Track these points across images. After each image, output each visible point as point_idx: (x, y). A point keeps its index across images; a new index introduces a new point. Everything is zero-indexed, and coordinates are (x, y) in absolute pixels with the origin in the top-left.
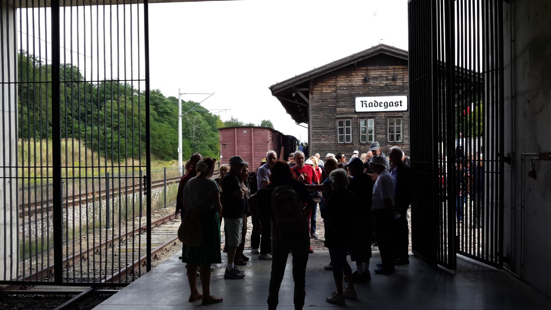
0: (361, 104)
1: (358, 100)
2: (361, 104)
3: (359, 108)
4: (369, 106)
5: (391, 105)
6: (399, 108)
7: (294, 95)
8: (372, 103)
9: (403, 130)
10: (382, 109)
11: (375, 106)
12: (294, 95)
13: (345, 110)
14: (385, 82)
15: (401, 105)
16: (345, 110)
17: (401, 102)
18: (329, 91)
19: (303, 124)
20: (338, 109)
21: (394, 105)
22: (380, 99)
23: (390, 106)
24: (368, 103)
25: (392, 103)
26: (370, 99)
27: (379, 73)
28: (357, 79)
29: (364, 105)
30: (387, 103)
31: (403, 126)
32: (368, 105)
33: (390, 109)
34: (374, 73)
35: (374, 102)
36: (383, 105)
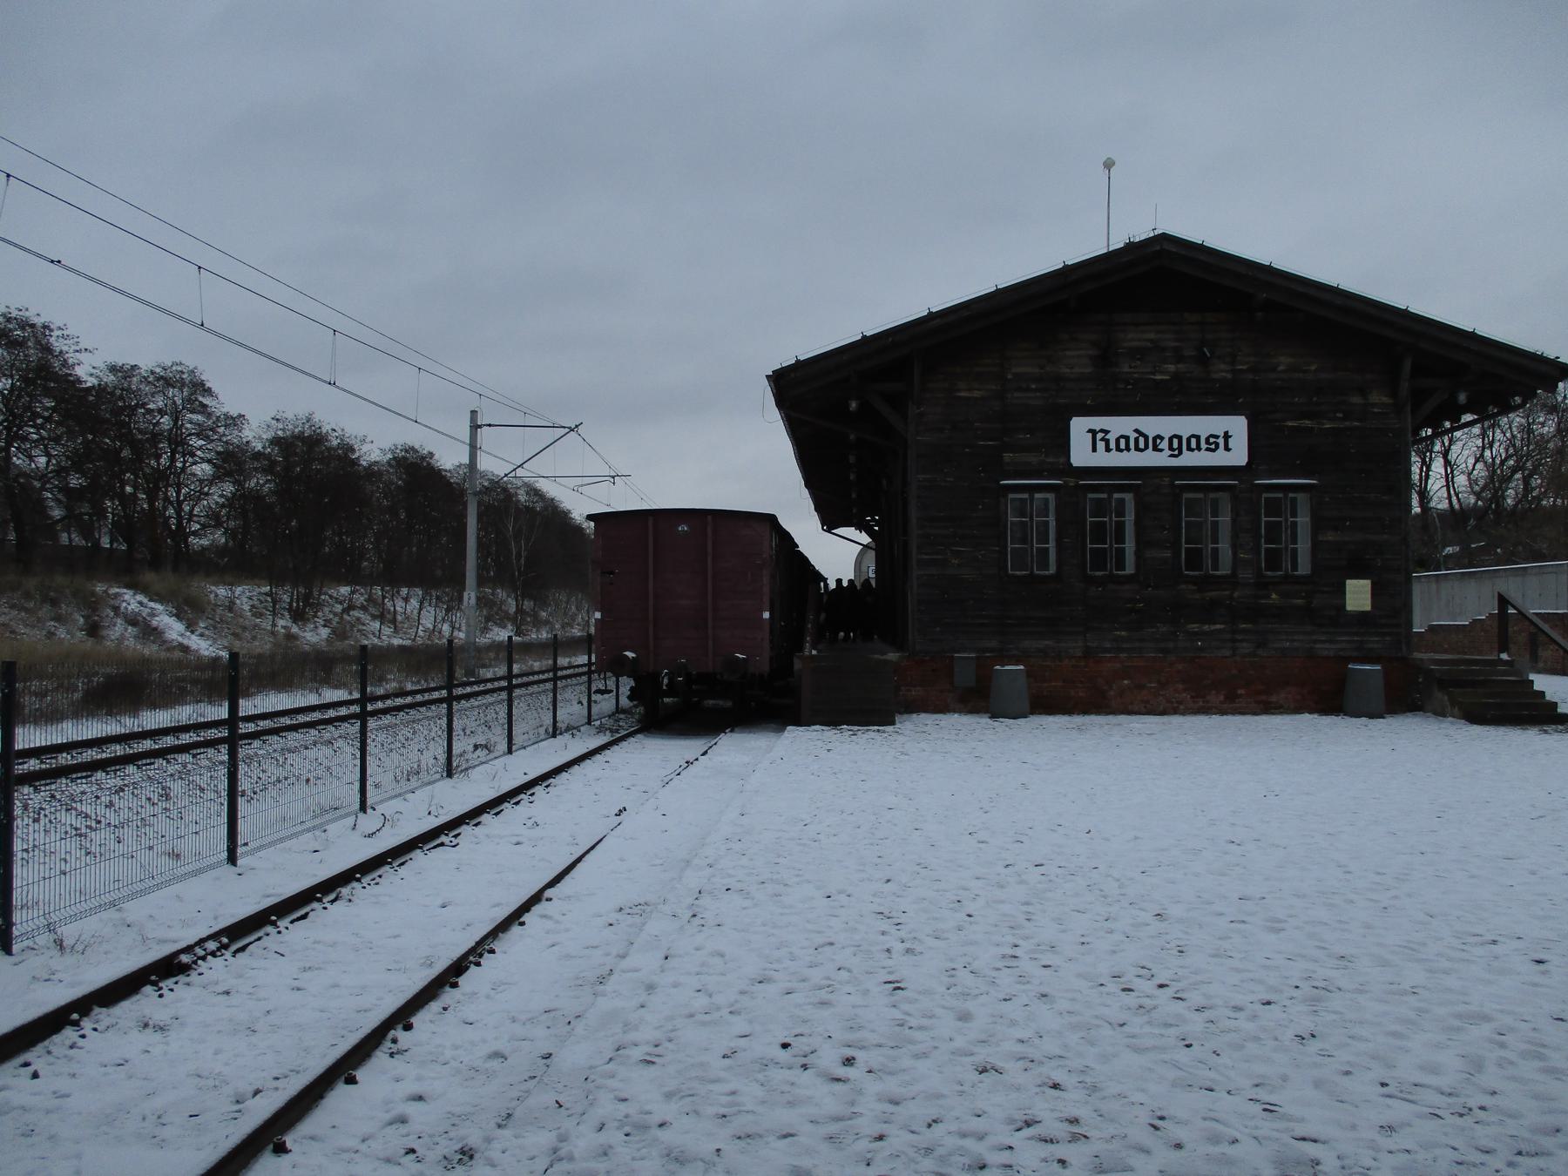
0: (1090, 442)
1: (1080, 427)
2: (1090, 442)
3: (1082, 454)
4: (1118, 449)
5: (1193, 445)
6: (1220, 459)
7: (854, 405)
8: (1127, 438)
9: (1235, 536)
10: (1162, 459)
11: (1137, 449)
12: (854, 405)
13: (1033, 459)
14: (1171, 368)
15: (1227, 449)
16: (1033, 459)
17: (1227, 436)
18: (977, 394)
19: (849, 532)
20: (1008, 456)
21: (1204, 446)
22: (1154, 425)
23: (1189, 449)
24: (1112, 437)
25: (1198, 438)
26: (1120, 425)
27: (1152, 336)
28: (1076, 360)
29: (1101, 445)
30: (1180, 438)
31: (1234, 521)
32: (1113, 445)
33: (1189, 459)
34: (1133, 338)
35: (1133, 436)
36: (1164, 445)
